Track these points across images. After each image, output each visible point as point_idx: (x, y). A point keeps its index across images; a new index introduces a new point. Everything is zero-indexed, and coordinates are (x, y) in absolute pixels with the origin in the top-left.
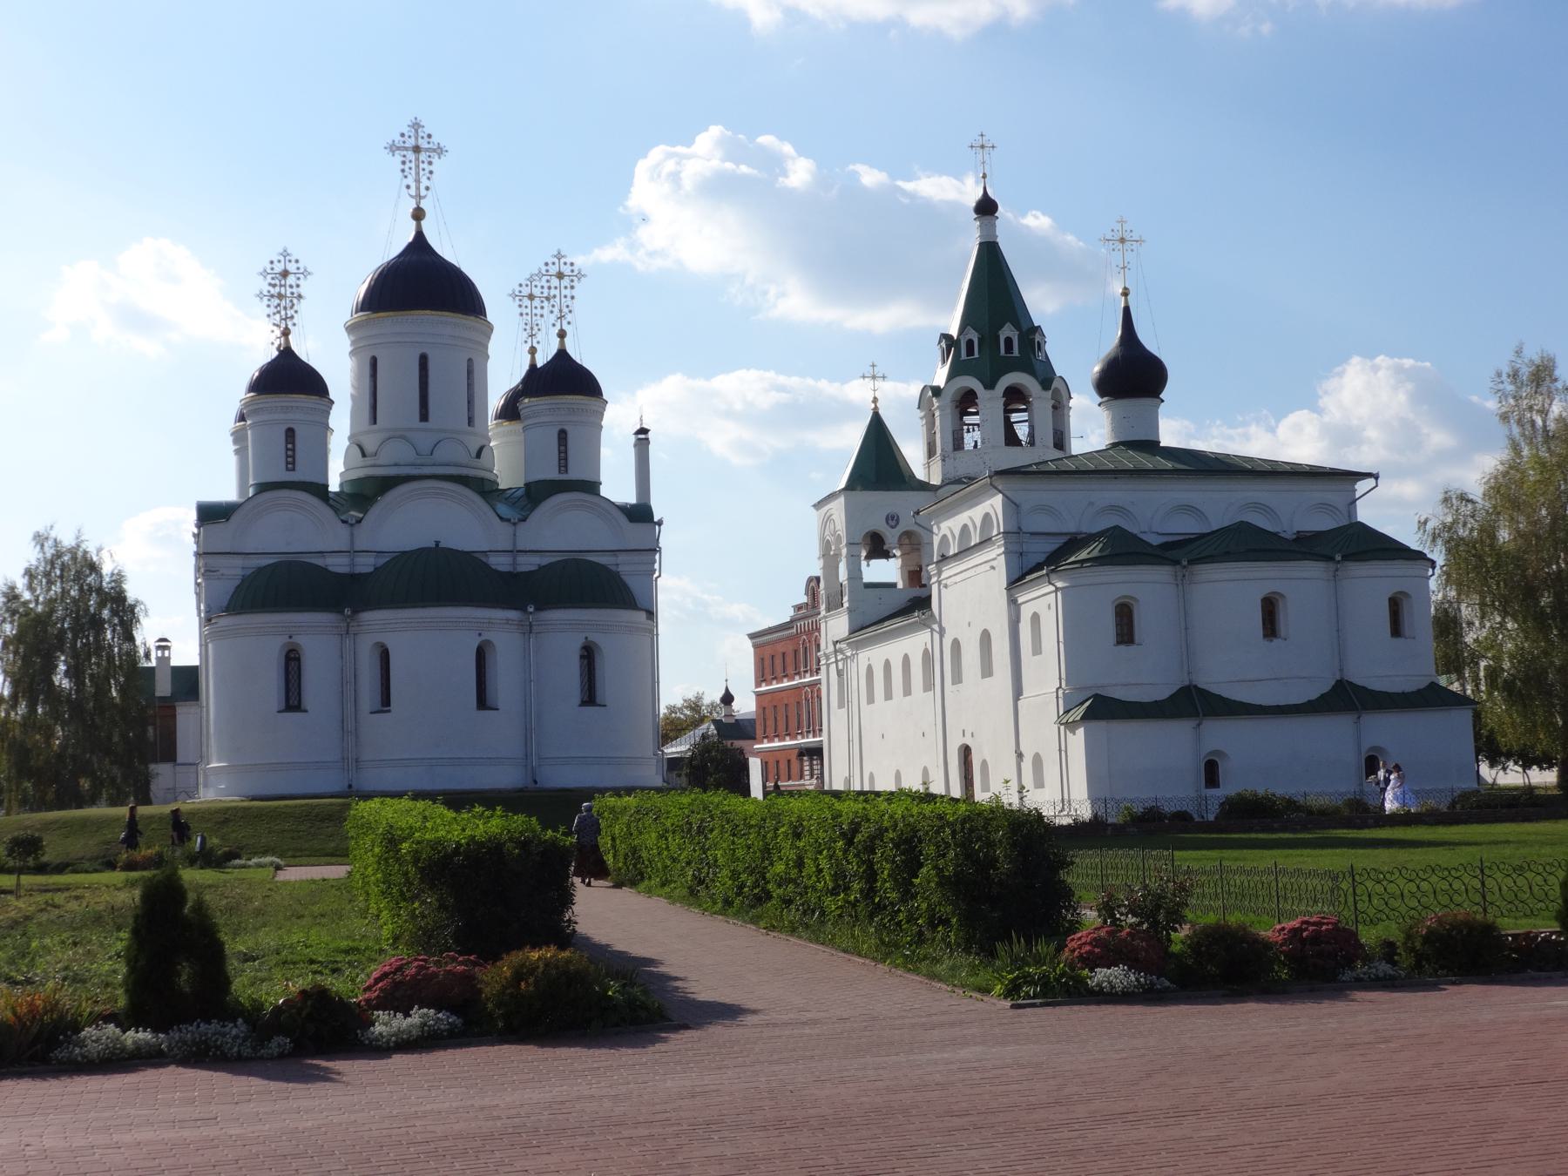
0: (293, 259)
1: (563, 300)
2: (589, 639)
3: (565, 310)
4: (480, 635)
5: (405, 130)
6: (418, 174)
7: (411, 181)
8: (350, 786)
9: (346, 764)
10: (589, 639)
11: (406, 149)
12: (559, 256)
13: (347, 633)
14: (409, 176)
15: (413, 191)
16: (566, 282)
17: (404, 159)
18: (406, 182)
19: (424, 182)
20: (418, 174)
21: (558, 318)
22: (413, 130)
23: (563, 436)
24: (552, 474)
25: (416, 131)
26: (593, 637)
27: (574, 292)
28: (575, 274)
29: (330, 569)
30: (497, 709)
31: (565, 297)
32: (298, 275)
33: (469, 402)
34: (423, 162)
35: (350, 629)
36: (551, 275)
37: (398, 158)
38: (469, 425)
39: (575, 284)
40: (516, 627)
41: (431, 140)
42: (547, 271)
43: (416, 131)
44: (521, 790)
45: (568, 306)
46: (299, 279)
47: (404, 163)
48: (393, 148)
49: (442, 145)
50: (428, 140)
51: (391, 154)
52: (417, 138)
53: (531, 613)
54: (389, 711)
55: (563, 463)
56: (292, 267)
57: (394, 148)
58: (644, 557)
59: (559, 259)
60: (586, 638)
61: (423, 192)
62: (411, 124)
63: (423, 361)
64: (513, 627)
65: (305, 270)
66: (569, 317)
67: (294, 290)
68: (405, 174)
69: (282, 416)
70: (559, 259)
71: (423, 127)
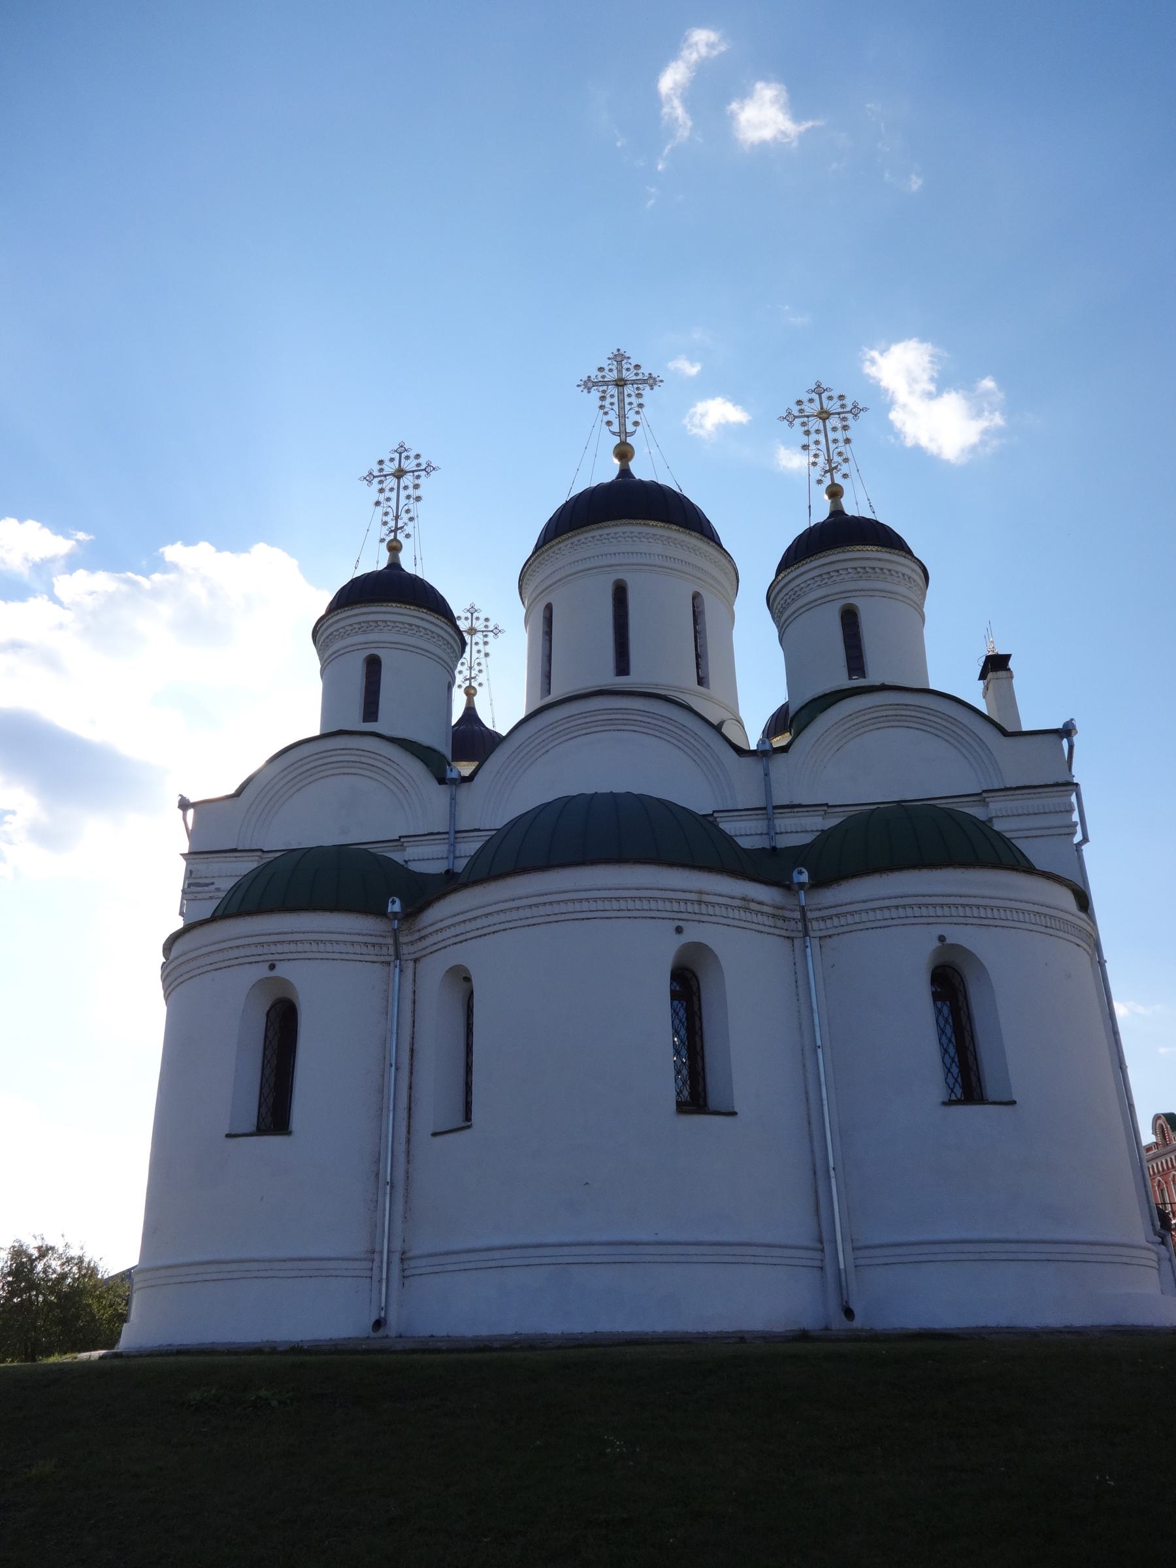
0: (412, 454)
1: (832, 446)
2: (949, 941)
3: (837, 459)
4: (679, 930)
5: (605, 364)
6: (622, 408)
7: (613, 416)
8: (378, 1324)
9: (376, 1264)
10: (949, 941)
11: (606, 383)
12: (819, 390)
13: (398, 956)
14: (611, 412)
15: (615, 428)
16: (834, 421)
17: (602, 395)
18: (606, 418)
19: (632, 417)
20: (622, 408)
21: (826, 472)
22: (615, 363)
23: (850, 619)
24: (841, 680)
25: (620, 363)
26: (959, 936)
27: (849, 434)
28: (848, 409)
29: (414, 867)
30: (734, 1114)
31: (835, 441)
32: (416, 474)
33: (698, 656)
34: (629, 395)
35: (405, 950)
36: (808, 417)
37: (595, 394)
38: (699, 684)
39: (850, 422)
40: (771, 921)
41: (639, 372)
42: (801, 411)
43: (620, 363)
44: (803, 1336)
45: (840, 454)
46: (418, 477)
47: (603, 398)
48: (588, 384)
49: (654, 375)
50: (635, 371)
51: (585, 391)
52: (620, 371)
53: (801, 885)
54: (469, 1127)
55: (855, 661)
56: (408, 465)
57: (590, 384)
58: (1050, 801)
59: (820, 395)
60: (942, 939)
61: (630, 428)
62: (611, 356)
63: (620, 594)
64: (760, 919)
65: (429, 465)
66: (844, 468)
67: (410, 491)
68: (606, 410)
69: (361, 638)
70: (820, 395)
71: (629, 358)
